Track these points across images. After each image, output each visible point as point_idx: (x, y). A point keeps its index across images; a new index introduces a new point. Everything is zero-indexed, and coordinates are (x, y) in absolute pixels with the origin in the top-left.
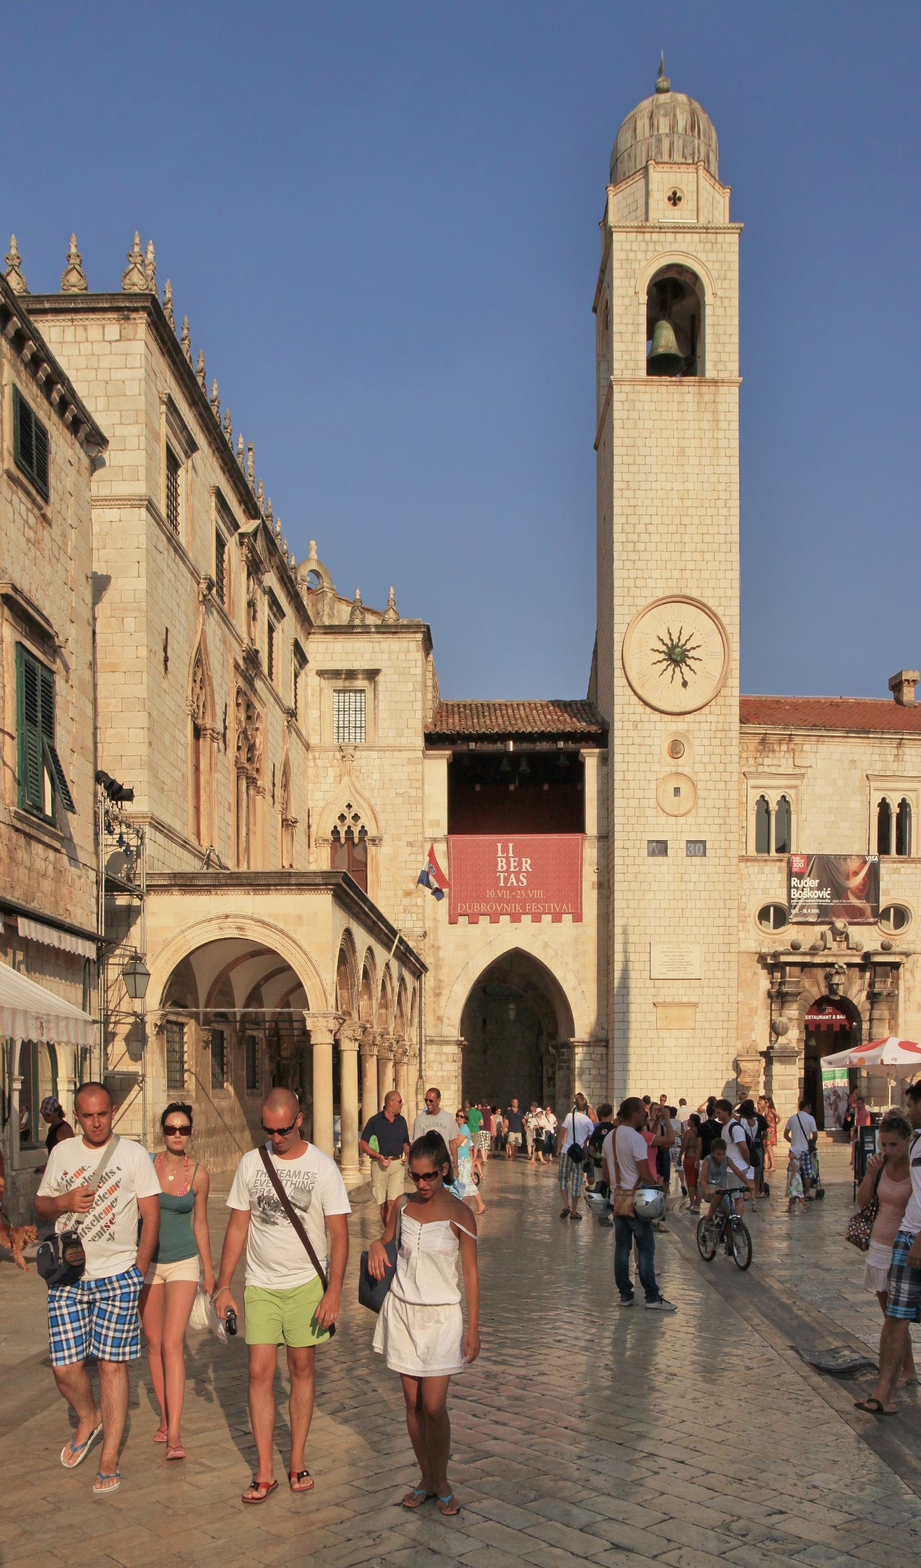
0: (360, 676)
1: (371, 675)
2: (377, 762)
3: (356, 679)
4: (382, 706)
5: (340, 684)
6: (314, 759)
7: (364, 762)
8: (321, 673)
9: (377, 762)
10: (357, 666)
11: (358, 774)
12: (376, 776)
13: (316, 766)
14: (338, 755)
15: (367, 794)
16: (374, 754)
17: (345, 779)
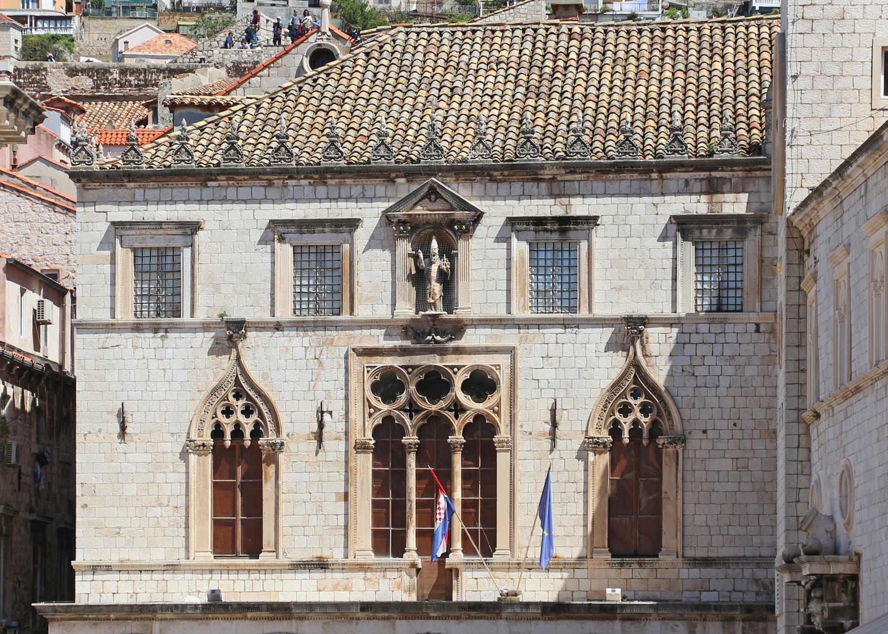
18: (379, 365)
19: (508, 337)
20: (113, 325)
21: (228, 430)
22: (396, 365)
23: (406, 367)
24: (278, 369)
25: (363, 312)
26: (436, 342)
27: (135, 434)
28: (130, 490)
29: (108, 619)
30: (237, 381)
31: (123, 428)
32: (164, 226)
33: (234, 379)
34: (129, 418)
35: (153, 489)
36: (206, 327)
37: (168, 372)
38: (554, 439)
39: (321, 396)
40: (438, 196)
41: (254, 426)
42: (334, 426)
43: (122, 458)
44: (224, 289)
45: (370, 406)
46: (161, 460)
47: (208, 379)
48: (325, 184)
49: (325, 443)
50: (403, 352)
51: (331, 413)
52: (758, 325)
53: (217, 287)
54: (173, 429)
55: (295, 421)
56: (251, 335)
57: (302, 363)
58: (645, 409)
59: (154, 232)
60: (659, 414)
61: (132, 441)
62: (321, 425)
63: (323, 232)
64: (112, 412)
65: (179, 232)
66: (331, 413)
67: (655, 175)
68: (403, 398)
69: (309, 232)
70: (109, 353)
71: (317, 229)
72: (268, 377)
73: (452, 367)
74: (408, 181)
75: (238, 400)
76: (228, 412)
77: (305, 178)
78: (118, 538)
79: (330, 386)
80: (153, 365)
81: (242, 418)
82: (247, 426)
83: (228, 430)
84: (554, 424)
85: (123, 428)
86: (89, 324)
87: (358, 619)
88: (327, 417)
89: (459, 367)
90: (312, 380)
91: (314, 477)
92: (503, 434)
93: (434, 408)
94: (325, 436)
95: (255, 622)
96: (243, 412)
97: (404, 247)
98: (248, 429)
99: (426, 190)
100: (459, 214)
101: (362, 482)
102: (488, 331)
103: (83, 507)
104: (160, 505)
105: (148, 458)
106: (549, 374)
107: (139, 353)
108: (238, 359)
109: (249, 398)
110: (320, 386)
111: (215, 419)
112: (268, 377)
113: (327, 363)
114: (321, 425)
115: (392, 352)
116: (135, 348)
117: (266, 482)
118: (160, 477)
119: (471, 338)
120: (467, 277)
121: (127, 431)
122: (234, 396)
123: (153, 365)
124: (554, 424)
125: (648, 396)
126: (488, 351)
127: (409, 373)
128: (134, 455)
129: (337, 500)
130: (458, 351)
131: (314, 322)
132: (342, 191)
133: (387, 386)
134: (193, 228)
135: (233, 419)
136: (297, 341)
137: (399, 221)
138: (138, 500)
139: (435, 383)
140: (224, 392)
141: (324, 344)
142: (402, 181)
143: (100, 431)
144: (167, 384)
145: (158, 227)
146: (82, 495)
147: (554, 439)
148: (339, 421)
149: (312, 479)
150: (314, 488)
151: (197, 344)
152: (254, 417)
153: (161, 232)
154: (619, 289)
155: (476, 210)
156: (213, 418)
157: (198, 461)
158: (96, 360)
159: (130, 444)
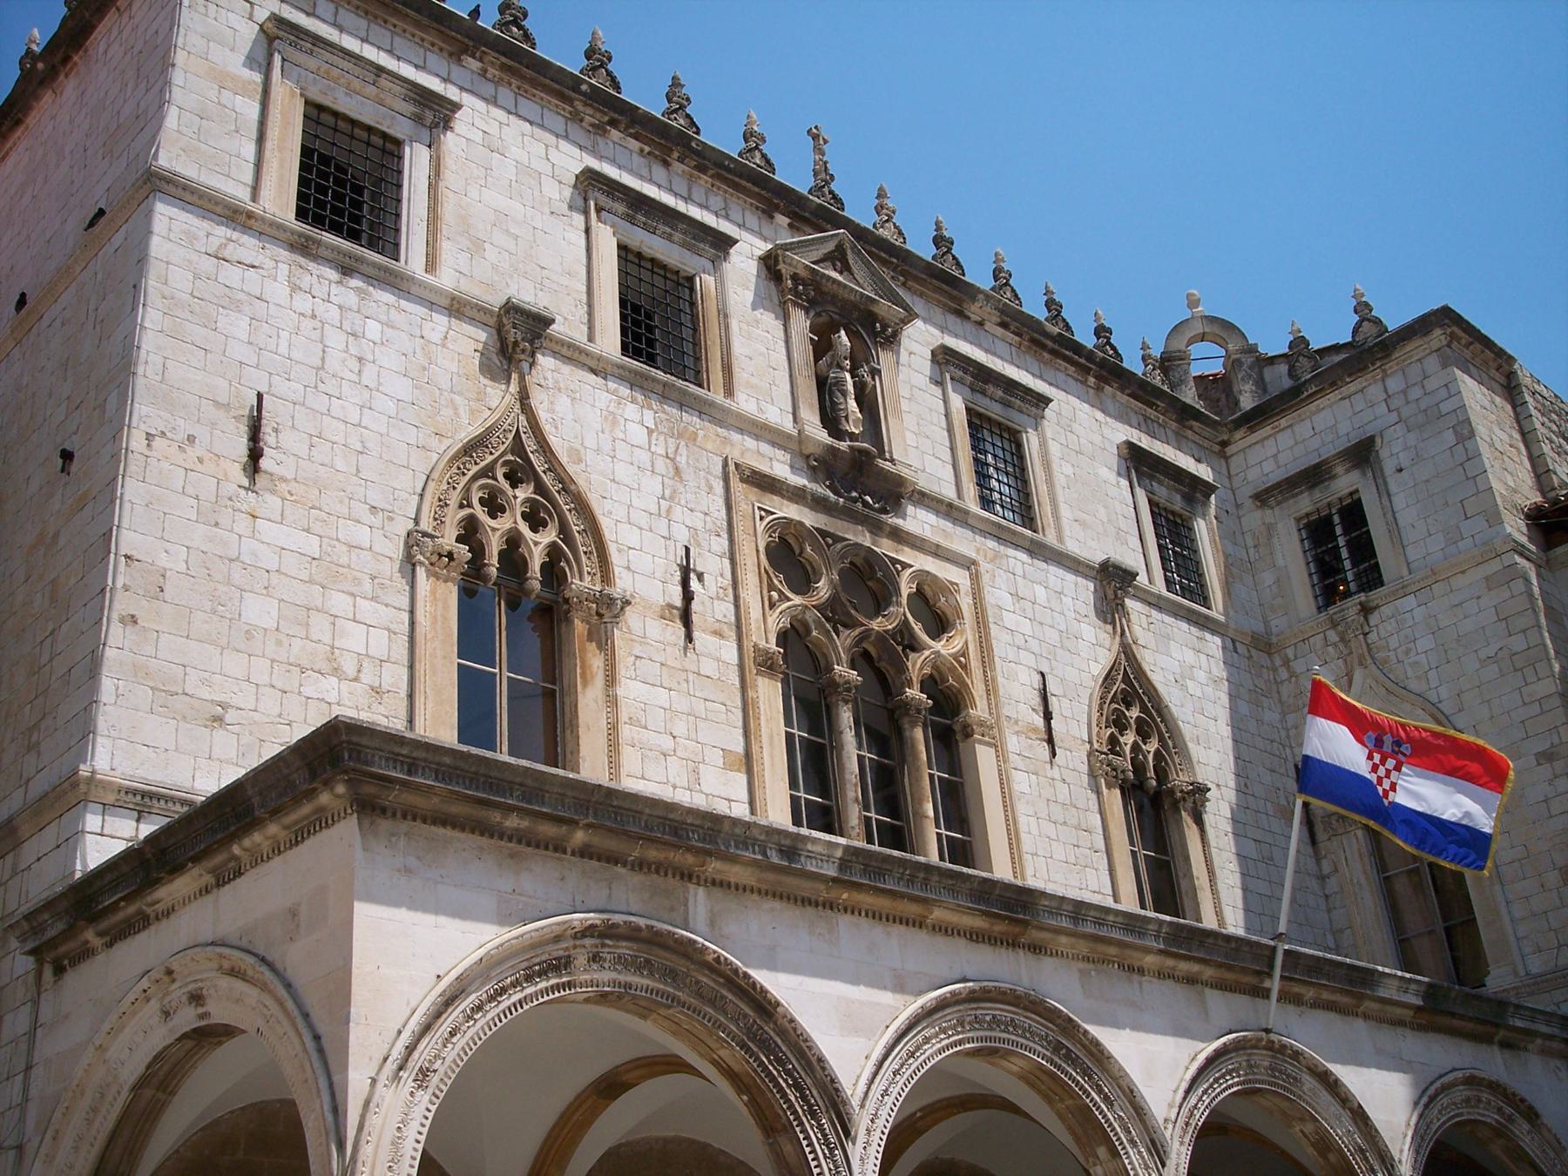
0: (1339, 470)
1: (1362, 453)
2: (1419, 613)
3: (1334, 477)
4: (1399, 502)
5: (1305, 503)
6: (1286, 663)
7: (1390, 626)
8: (1263, 498)
9: (1419, 613)
10: (1328, 452)
11: (1381, 655)
12: (1425, 643)
13: (1292, 674)
14: (1333, 636)
15: (1414, 685)
16: (1410, 601)
17: (1358, 675)
18: (780, 514)
19: (962, 541)
20: (250, 215)
21: (494, 546)
22: (808, 523)
23: (824, 534)
24: (598, 451)
25: (744, 402)
26: (865, 504)
27: (283, 479)
28: (259, 611)
29: (559, 847)
30: (518, 447)
31: (255, 455)
32: (384, 82)
33: (511, 436)
34: (268, 437)
35: (320, 627)
36: (457, 307)
37: (369, 373)
38: (1050, 741)
39: (683, 536)
40: (845, 268)
41: (548, 555)
42: (711, 606)
43: (243, 524)
44: (491, 253)
45: (771, 587)
46: (344, 560)
47: (457, 414)
48: (666, 164)
49: (696, 634)
50: (819, 504)
51: (700, 577)
52: (1233, 641)
53: (476, 247)
54: (375, 498)
55: (640, 568)
56: (545, 361)
57: (644, 457)
58: (1143, 732)
59: (357, 84)
60: (1161, 739)
61: (273, 492)
62: (688, 596)
63: (669, 238)
64: (226, 407)
65: (409, 108)
66: (700, 577)
67: (1092, 380)
68: (823, 589)
69: (645, 227)
70: (232, 275)
71: (662, 228)
72: (580, 461)
73: (894, 561)
74: (790, 225)
75: (514, 486)
76: (494, 506)
77: (636, 137)
78: (219, 734)
79: (697, 521)
80: (336, 340)
81: (524, 528)
82: (538, 545)
83: (494, 546)
84: (1048, 716)
85: (255, 455)
86: (193, 191)
87: (1141, 971)
88: (694, 584)
89: (905, 566)
90: (663, 497)
91: (681, 704)
92: (979, 710)
93: (877, 624)
94: (695, 618)
95: (940, 941)
96: (525, 516)
97: (800, 322)
98: (537, 560)
99: (831, 246)
100: (884, 308)
101: (771, 737)
102: (931, 518)
103: (122, 620)
104: (337, 671)
105: (312, 545)
106: (1026, 626)
107: (303, 303)
108: (524, 397)
109: (540, 488)
110: (678, 511)
111: (468, 511)
112: (580, 461)
113: (688, 474)
114: (688, 596)
115: (797, 495)
116: (295, 288)
117: (585, 684)
118: (339, 602)
119: (917, 521)
120: (899, 413)
121: (264, 463)
122: (506, 476)
123: (336, 340)
124: (1048, 716)
125: (1144, 709)
126: (937, 552)
127: (829, 546)
128: (275, 534)
129: (728, 766)
130: (898, 536)
131: (665, 385)
132: (694, 190)
133: (788, 557)
134: (435, 114)
135: (504, 523)
136: (631, 411)
137: (795, 277)
138: (279, 643)
139: (869, 581)
140: (490, 458)
141: (680, 436)
142: (782, 220)
143: (191, 439)
144: (366, 394)
145: (371, 77)
146: (126, 588)
147: (1050, 741)
148: (718, 598)
149: (675, 706)
150: (680, 728)
151: (436, 337)
152: (549, 536)
153: (371, 90)
154: (1083, 524)
155: (906, 308)
156: (461, 506)
157: (433, 592)
158: (197, 277)
159: (268, 497)
